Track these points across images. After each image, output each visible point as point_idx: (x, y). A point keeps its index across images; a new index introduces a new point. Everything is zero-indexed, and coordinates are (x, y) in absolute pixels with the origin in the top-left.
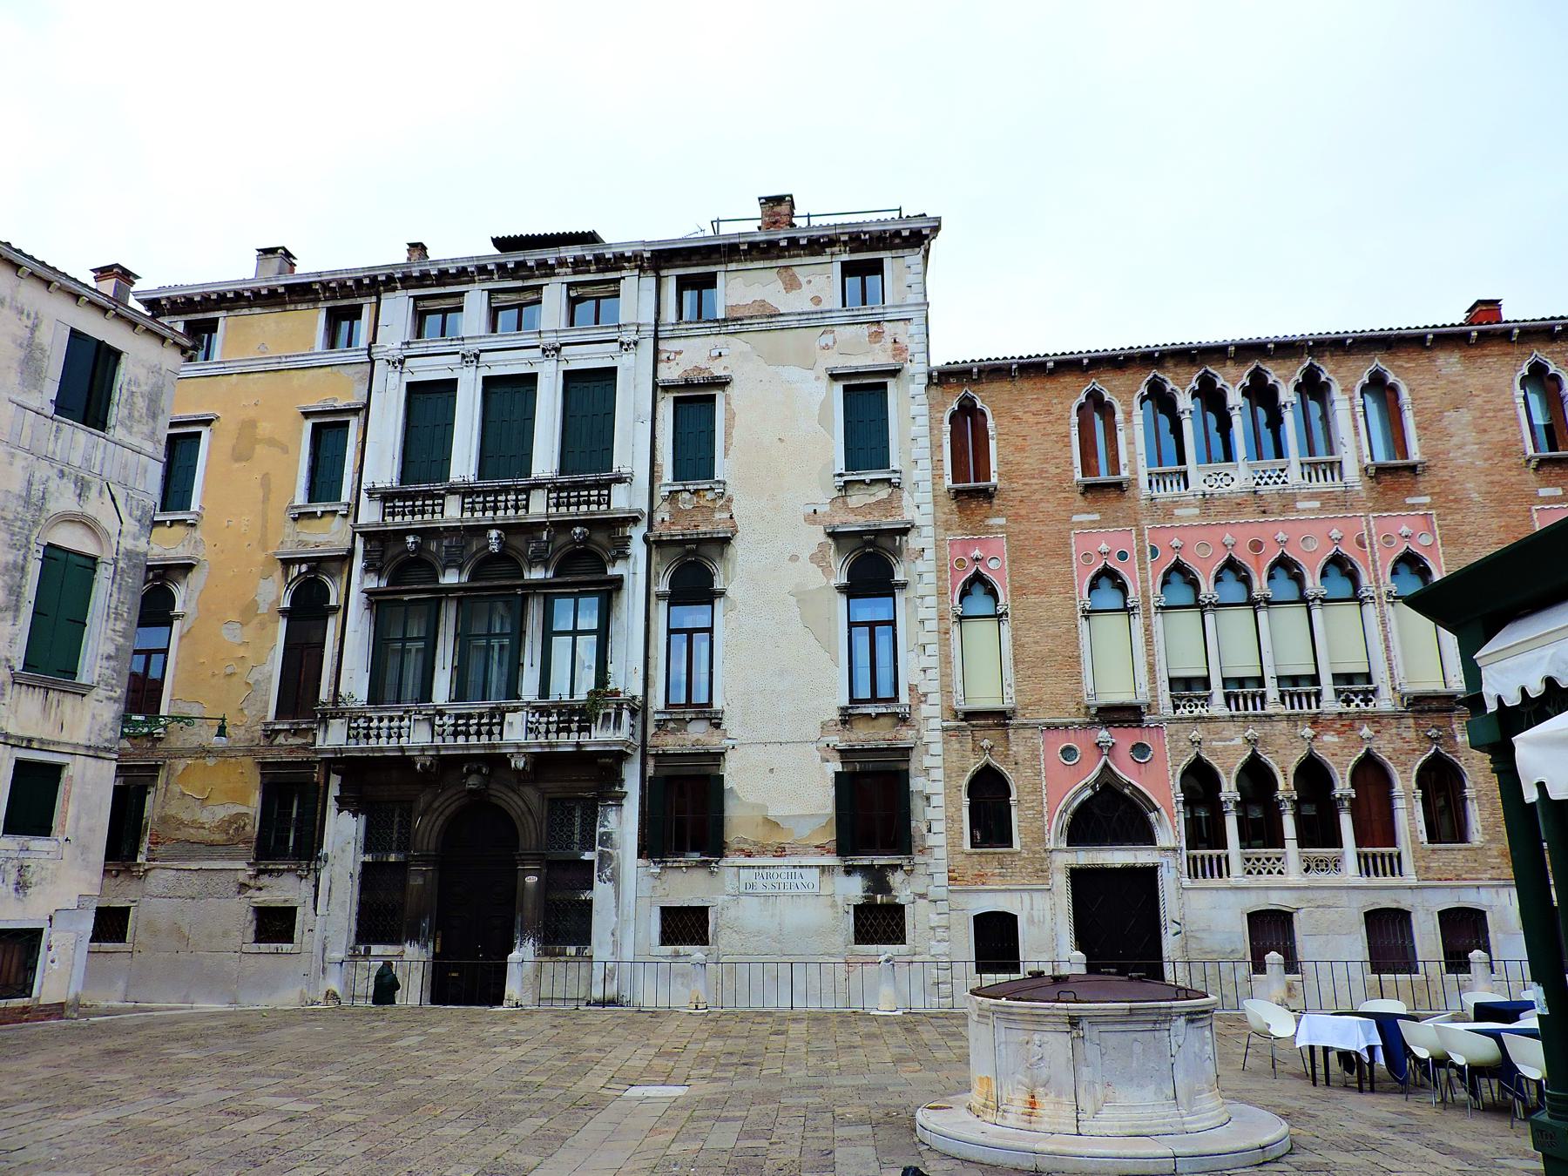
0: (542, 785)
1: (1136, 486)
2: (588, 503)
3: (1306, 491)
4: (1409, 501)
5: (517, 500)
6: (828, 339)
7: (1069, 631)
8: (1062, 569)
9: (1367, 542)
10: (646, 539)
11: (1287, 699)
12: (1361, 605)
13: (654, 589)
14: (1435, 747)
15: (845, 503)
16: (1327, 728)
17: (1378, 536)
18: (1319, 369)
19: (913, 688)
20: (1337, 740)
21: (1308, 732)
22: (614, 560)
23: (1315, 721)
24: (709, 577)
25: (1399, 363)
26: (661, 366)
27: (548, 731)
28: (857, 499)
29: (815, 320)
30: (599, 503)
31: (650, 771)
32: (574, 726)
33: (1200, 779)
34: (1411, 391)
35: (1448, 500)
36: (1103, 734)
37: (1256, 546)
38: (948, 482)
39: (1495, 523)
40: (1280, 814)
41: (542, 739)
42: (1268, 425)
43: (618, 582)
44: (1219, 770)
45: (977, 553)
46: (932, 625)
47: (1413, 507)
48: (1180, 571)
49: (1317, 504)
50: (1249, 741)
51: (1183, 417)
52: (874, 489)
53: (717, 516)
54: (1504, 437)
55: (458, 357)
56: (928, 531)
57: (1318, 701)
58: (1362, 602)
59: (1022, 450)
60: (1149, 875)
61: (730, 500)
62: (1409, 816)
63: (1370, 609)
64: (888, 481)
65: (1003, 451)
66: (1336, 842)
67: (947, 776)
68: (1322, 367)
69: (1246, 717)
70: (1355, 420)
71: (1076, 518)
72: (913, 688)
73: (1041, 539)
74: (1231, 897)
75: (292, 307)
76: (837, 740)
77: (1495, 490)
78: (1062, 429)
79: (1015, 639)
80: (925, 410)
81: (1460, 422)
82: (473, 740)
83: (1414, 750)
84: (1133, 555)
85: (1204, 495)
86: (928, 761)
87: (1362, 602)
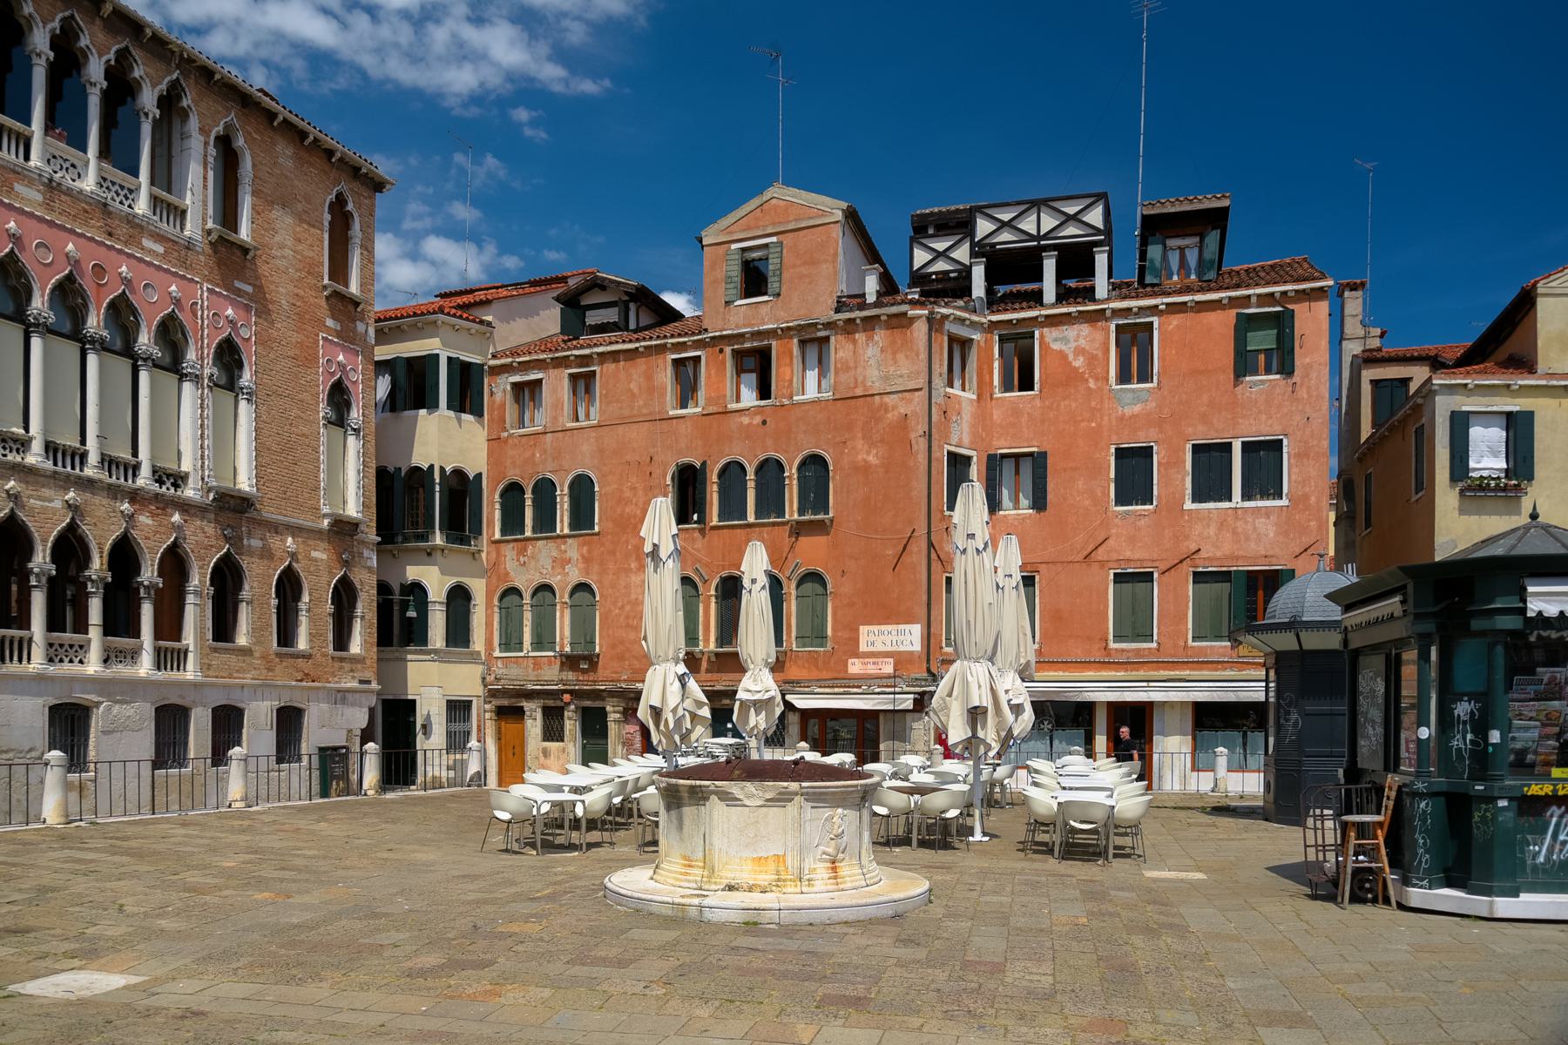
3: (153, 228)
4: (238, 284)
9: (199, 313)
11: (106, 465)
12: (180, 381)
14: (227, 546)
17: (209, 312)
18: (183, 90)
20: (149, 521)
21: (126, 506)
25: (249, 129)
34: (254, 165)
39: (296, 337)
40: (87, 595)
44: (36, 535)
47: (239, 292)
49: (160, 249)
50: (70, 506)
51: (35, 60)
54: (311, 254)
57: (134, 475)
63: (187, 387)
66: (136, 634)
68: (187, 90)
69: (68, 476)
77: (298, 304)
83: (211, 546)
85: (51, 180)
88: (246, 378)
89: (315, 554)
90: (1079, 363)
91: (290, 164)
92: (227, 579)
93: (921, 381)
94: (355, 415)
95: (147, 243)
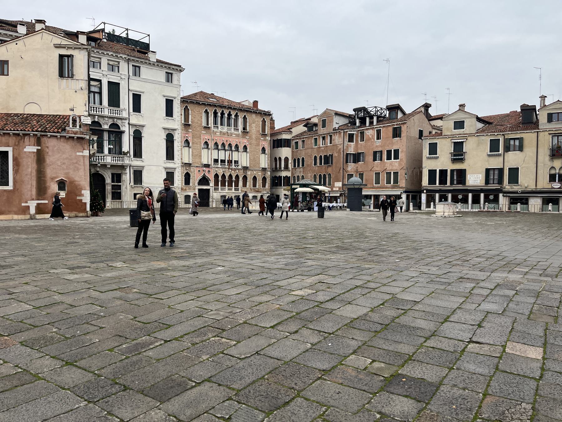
23: (231, 169)
33: (216, 176)
35: (251, 137)
36: (204, 169)
37: (227, 141)
38: (183, 122)
40: (226, 182)
45: (187, 136)
48: (216, 144)
56: (180, 130)
58: (239, 152)
59: (194, 118)
60: (209, 190)
62: (241, 183)
63: (240, 153)
74: (219, 193)
79: (192, 152)
81: (254, 125)
84: (210, 140)
87: (239, 152)
88: (248, 150)
90: (371, 136)
92: (245, 178)
93: (342, 142)
94: (266, 152)
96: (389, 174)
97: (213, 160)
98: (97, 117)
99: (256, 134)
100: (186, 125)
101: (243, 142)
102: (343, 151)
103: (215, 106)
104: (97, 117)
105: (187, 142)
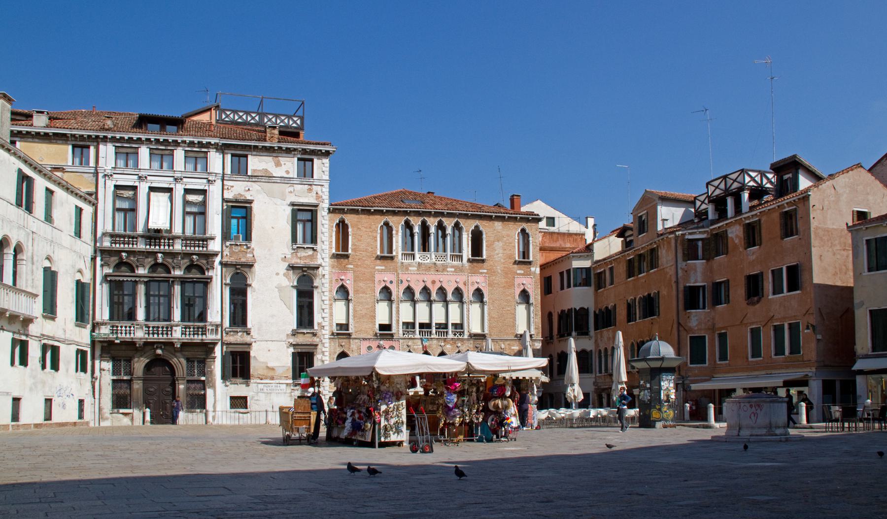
0: (184, 353)
1: (398, 258)
2: (199, 247)
4: (481, 271)
5: (169, 243)
6: (291, 189)
7: (372, 307)
8: (372, 285)
10: (221, 263)
13: (224, 282)
15: (296, 255)
16: (448, 343)
19: (319, 324)
21: (443, 344)
22: (208, 269)
24: (246, 279)
26: (225, 191)
27: (190, 334)
28: (302, 253)
29: (285, 180)
30: (203, 247)
31: (225, 349)
32: (200, 333)
34: (486, 233)
35: (491, 272)
36: (382, 342)
38: (334, 251)
39: (503, 280)
41: (188, 337)
42: (442, 237)
43: (211, 278)
45: (343, 277)
46: (327, 302)
47: (482, 273)
48: (409, 291)
49: (453, 270)
52: (308, 250)
53: (248, 255)
55: (136, 177)
56: (327, 268)
59: (360, 240)
61: (253, 249)
64: (313, 248)
65: (354, 241)
67: (330, 354)
70: (468, 242)
71: (377, 268)
72: (319, 324)
73: (364, 274)
75: (55, 141)
76: (292, 340)
78: (375, 235)
80: (327, 222)
82: (161, 336)
86: (324, 349)
89: (513, 348)
91: (501, 227)
95: (448, 269)
96: (778, 330)
97: (401, 324)
98: (160, 255)
99: (504, 263)
100: (341, 255)
101: (479, 280)
102: (677, 282)
103: (405, 213)
104: (160, 255)
105: (343, 290)
